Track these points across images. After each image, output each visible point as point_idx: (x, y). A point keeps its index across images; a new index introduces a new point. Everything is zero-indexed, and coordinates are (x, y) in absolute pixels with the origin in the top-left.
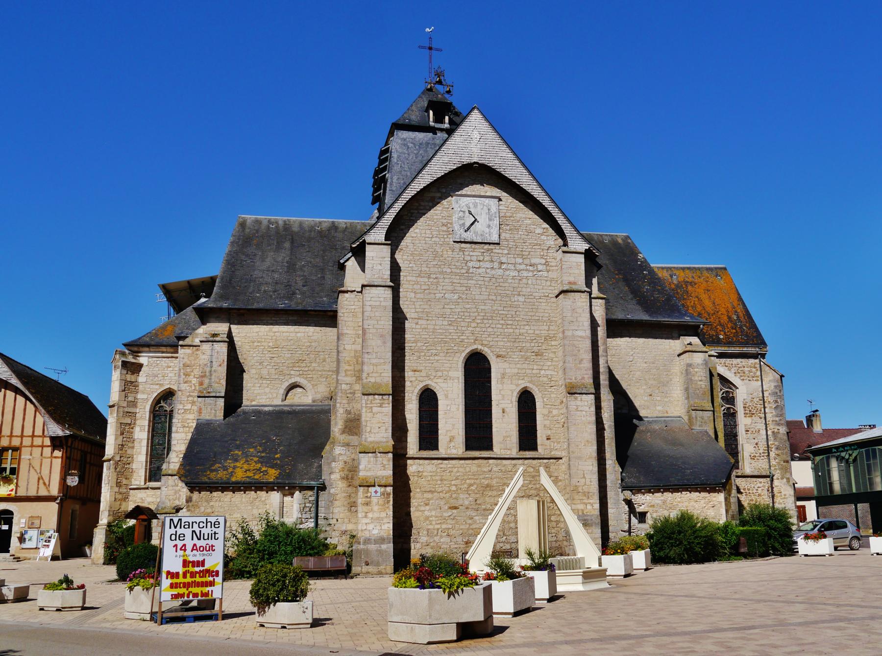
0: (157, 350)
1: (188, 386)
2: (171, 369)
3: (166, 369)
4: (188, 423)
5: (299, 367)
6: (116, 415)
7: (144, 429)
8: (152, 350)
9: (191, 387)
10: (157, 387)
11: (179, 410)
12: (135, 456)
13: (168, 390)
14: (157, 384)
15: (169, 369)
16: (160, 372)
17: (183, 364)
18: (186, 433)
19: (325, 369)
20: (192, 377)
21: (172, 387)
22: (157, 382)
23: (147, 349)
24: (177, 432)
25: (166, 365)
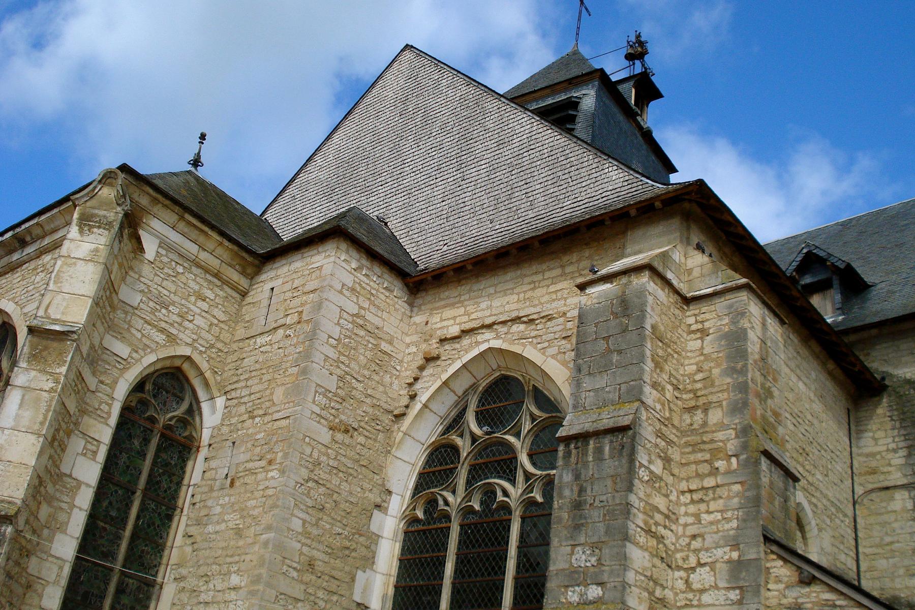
0: (194, 234)
1: (659, 401)
2: (205, 306)
3: (193, 299)
4: (657, 524)
5: (803, 466)
6: (64, 370)
7: (95, 453)
8: (181, 225)
9: (663, 405)
10: (160, 338)
11: (641, 465)
12: (46, 532)
13: (177, 363)
14: (162, 331)
15: (200, 303)
16: (176, 299)
17: (653, 327)
18: (652, 555)
19: (830, 494)
20: (666, 377)
21: (196, 358)
22: (163, 325)
23: (172, 218)
24: (637, 544)
25: (197, 287)
